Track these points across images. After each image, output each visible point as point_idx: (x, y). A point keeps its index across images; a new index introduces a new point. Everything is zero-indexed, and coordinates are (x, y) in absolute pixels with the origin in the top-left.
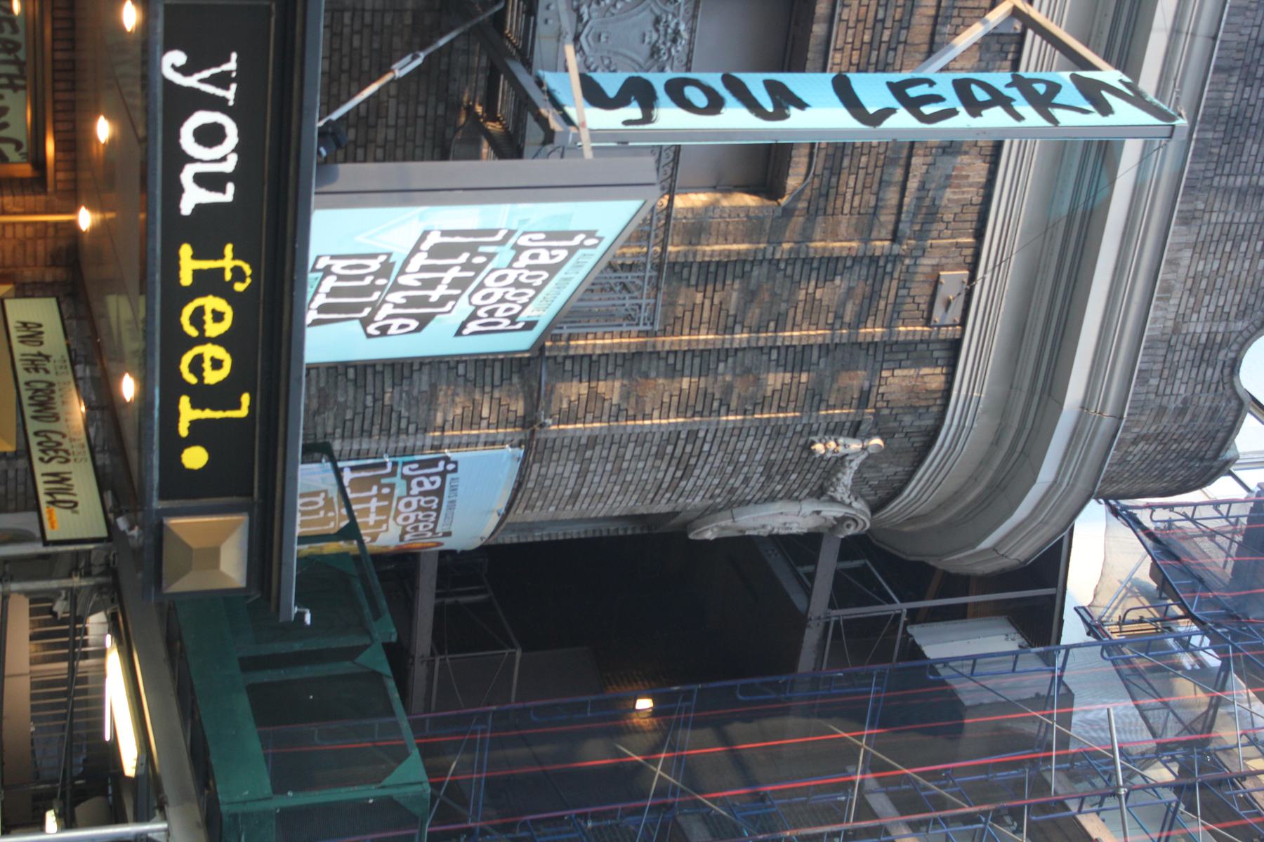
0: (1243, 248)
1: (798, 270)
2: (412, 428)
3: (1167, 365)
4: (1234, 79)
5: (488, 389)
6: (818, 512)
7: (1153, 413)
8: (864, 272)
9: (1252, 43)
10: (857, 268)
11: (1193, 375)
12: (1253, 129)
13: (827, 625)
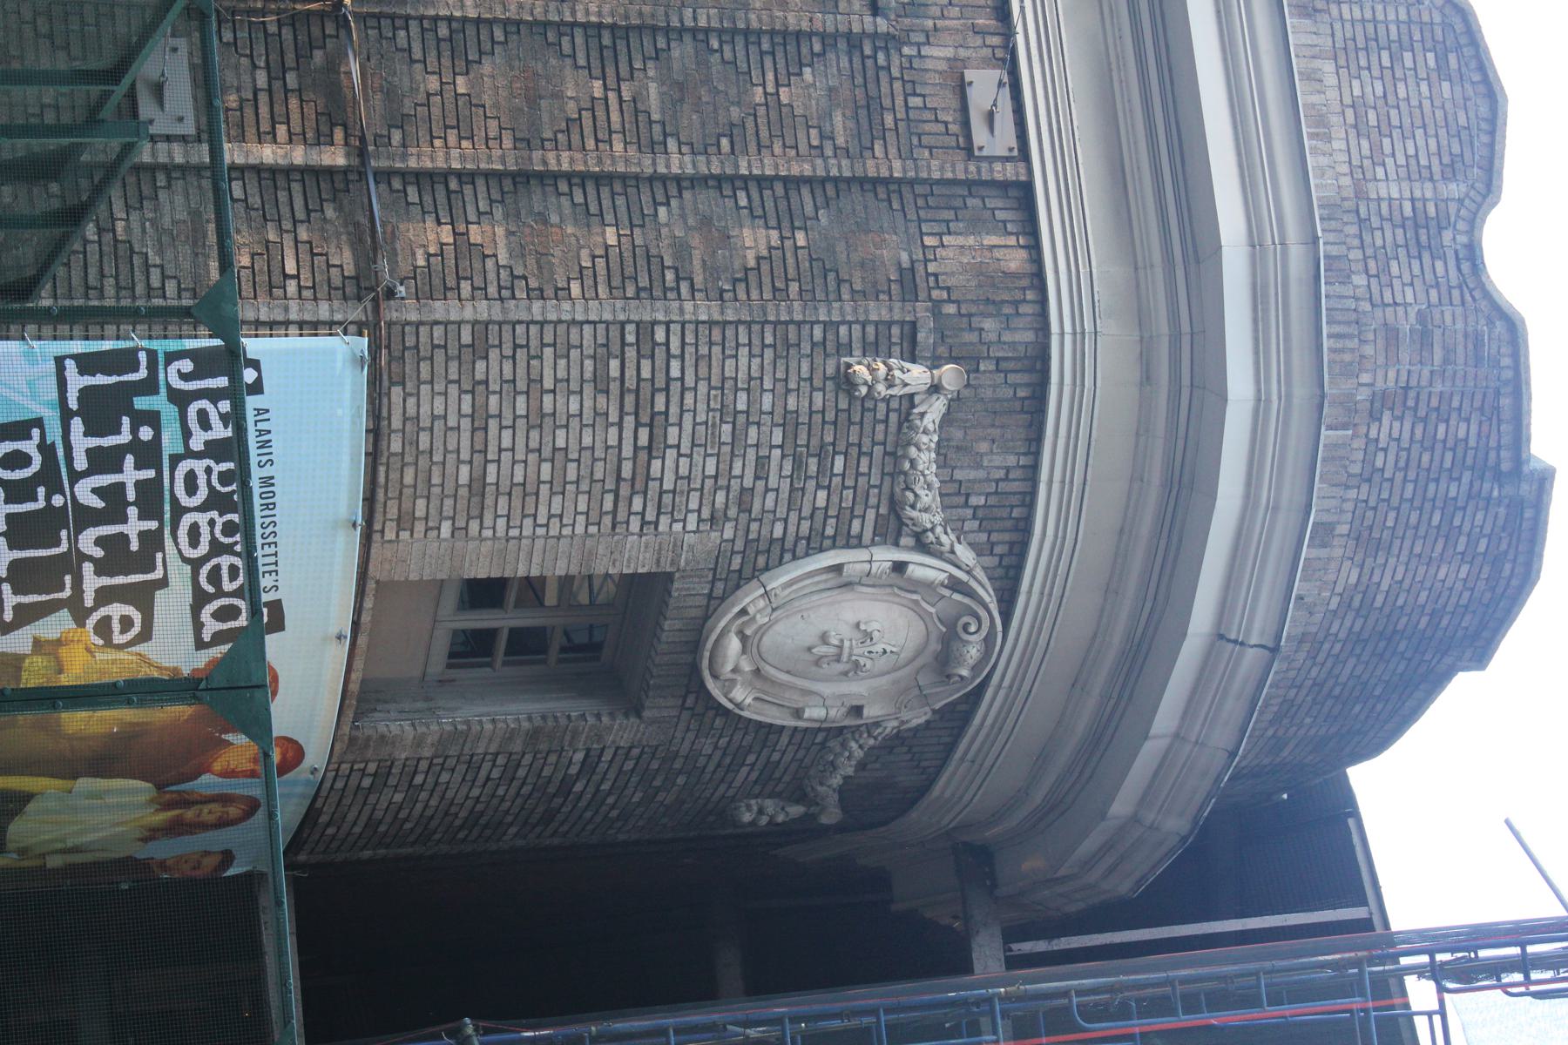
0: (1409, 63)
1: (741, 54)
3: (1369, 252)
5: (287, 225)
6: (899, 567)
7: (1381, 342)
8: (844, 62)
10: (831, 56)
11: (1416, 271)
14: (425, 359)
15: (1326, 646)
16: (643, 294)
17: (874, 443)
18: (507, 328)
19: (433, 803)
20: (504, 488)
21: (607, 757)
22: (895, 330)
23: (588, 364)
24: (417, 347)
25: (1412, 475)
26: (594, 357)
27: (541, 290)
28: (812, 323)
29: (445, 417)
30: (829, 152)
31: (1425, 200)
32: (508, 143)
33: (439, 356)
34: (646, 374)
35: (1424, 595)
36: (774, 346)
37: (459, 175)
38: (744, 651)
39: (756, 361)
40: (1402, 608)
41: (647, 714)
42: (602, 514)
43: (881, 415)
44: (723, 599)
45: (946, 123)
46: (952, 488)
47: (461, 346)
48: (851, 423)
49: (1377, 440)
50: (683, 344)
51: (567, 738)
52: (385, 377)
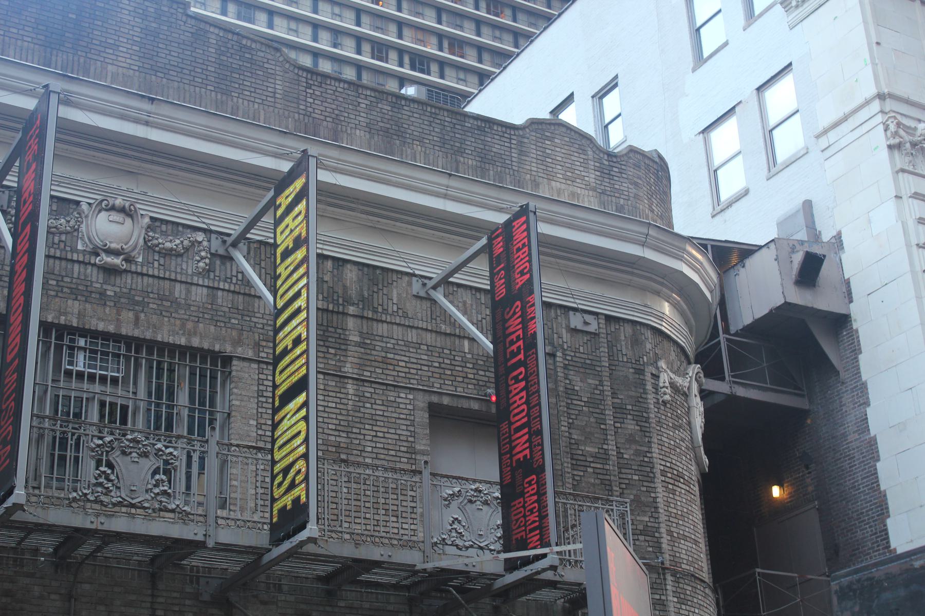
0: (549, 152)
4: (462, 159)
8: (572, 373)
9: (443, 149)
10: (570, 377)
12: (487, 148)
13: (734, 382)
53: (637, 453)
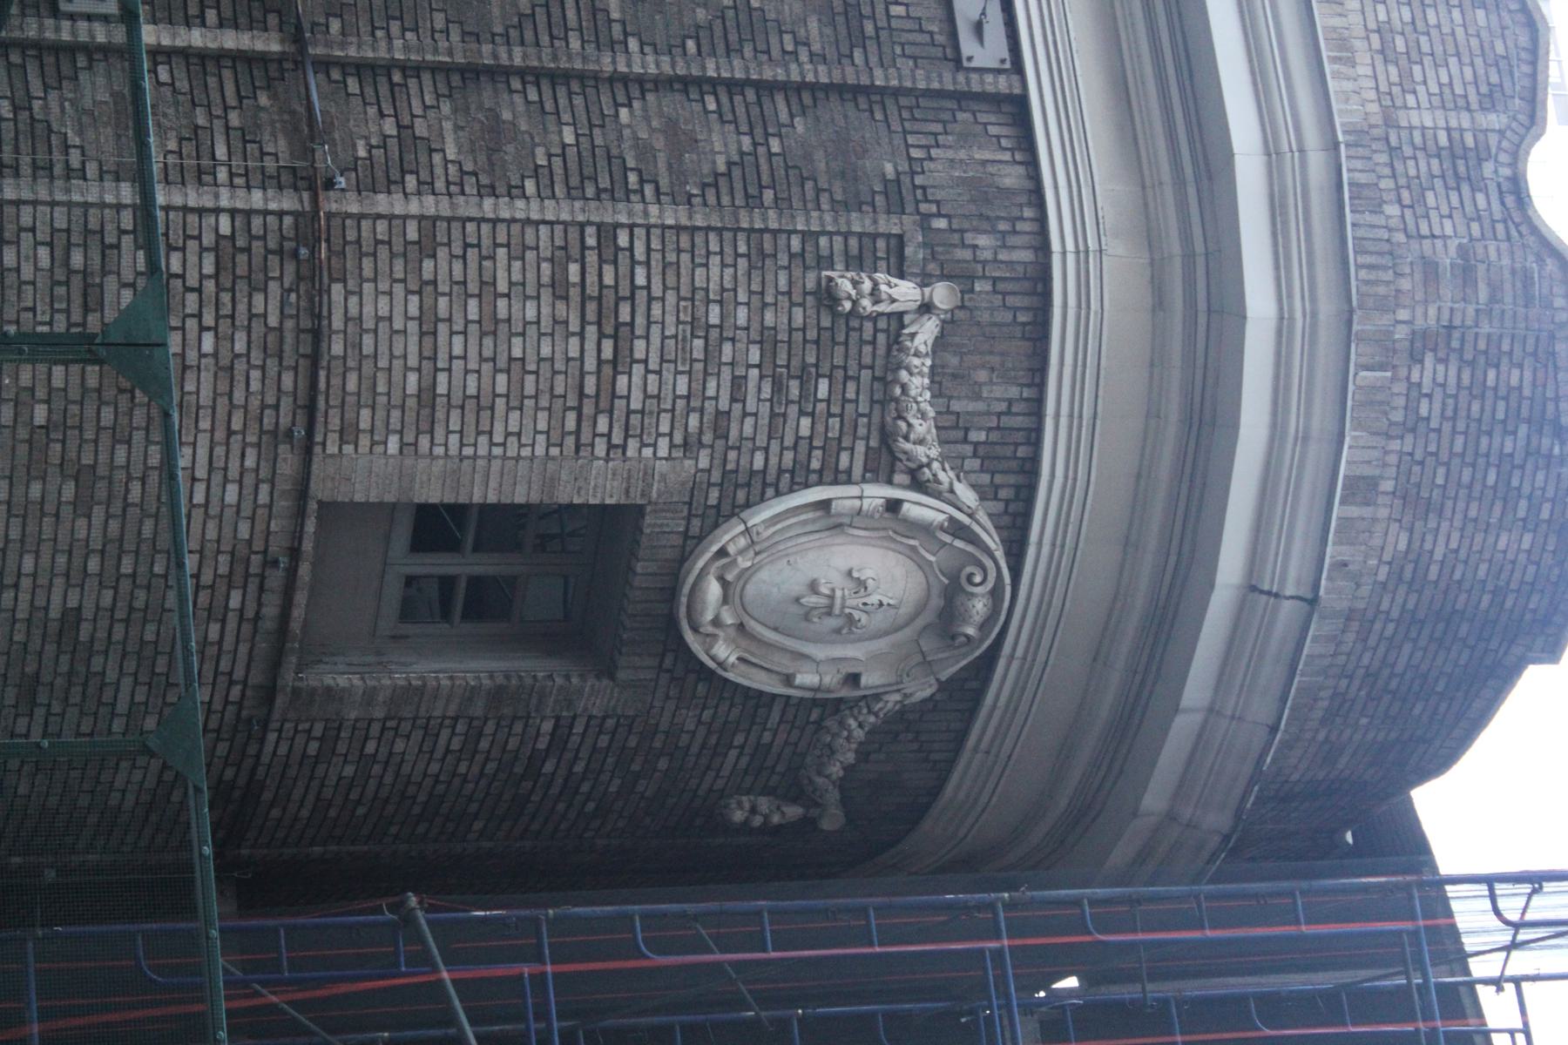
2: (92, 169)
3: (1402, 181)
5: (218, 111)
6: (893, 506)
7: (1418, 276)
11: (1455, 201)
14: (367, 255)
15: (1378, 626)
16: (603, 196)
17: (861, 367)
18: (456, 225)
19: (388, 779)
20: (457, 399)
21: (579, 728)
22: (881, 244)
23: (546, 267)
24: (358, 241)
25: (1461, 426)
26: (552, 260)
27: (493, 187)
28: (790, 233)
29: (390, 319)
30: (804, 57)
31: (1461, 130)
32: (455, 36)
33: (383, 252)
34: (609, 279)
35: (1483, 567)
36: (748, 256)
37: (404, 67)
38: (725, 600)
39: (729, 271)
40: (1459, 582)
41: (622, 675)
42: (564, 434)
43: (867, 335)
44: (700, 538)
45: (931, 33)
46: (948, 421)
47: (407, 243)
48: (834, 342)
49: (1419, 385)
50: (649, 249)
51: (534, 701)
52: (325, 274)
53: (645, 151)
